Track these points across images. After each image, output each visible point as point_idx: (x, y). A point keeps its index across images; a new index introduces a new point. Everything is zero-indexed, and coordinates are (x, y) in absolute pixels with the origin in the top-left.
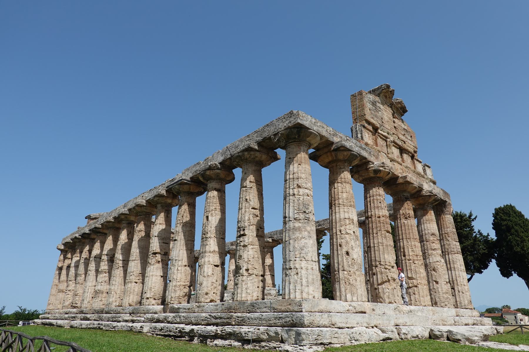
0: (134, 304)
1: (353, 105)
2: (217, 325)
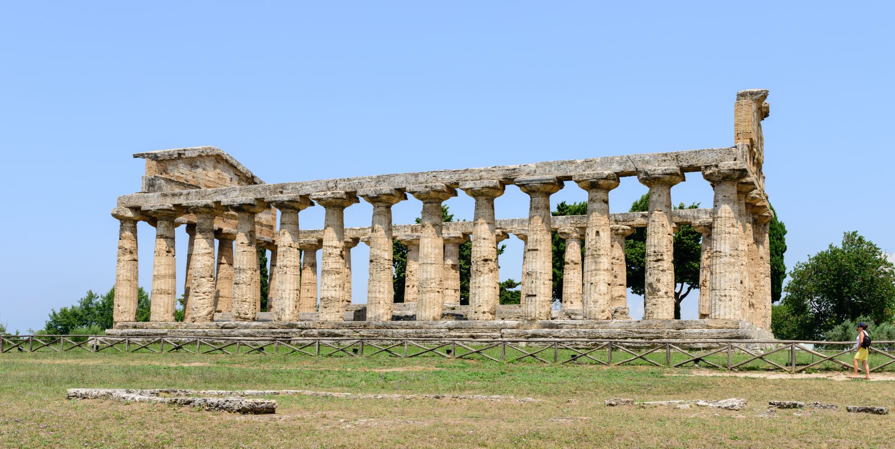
0: (439, 318)
1: (736, 116)
2: (642, 338)
